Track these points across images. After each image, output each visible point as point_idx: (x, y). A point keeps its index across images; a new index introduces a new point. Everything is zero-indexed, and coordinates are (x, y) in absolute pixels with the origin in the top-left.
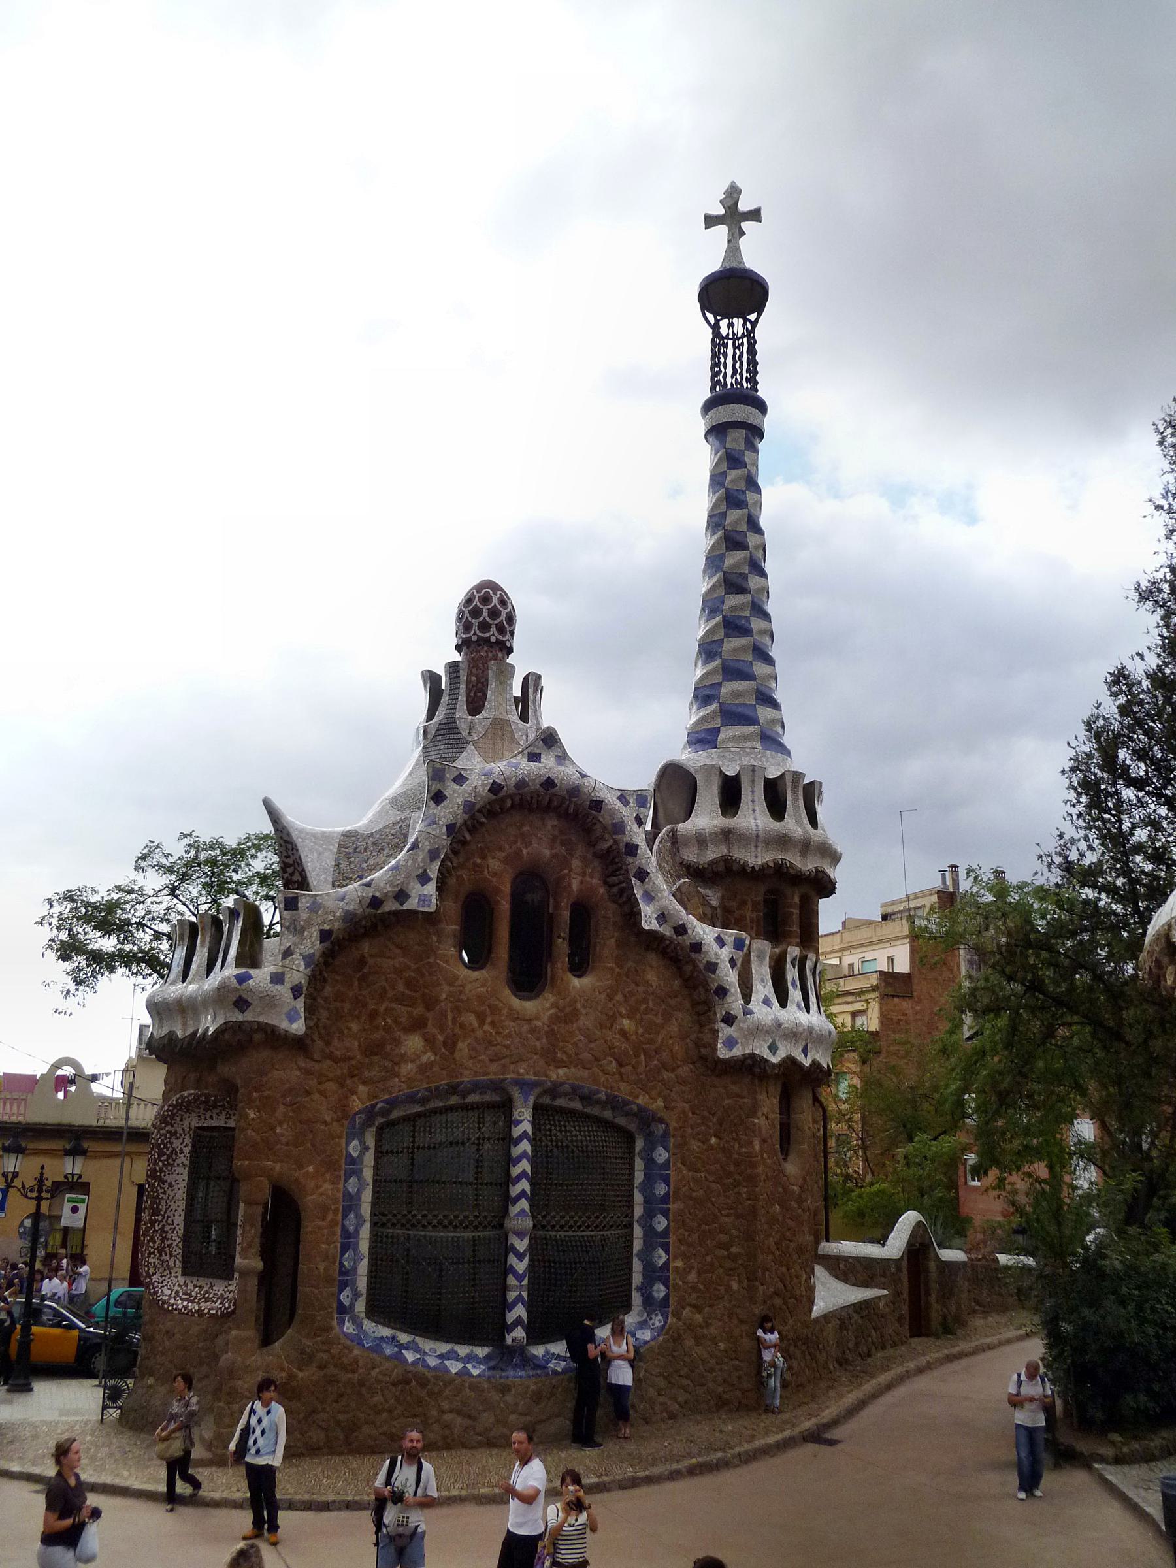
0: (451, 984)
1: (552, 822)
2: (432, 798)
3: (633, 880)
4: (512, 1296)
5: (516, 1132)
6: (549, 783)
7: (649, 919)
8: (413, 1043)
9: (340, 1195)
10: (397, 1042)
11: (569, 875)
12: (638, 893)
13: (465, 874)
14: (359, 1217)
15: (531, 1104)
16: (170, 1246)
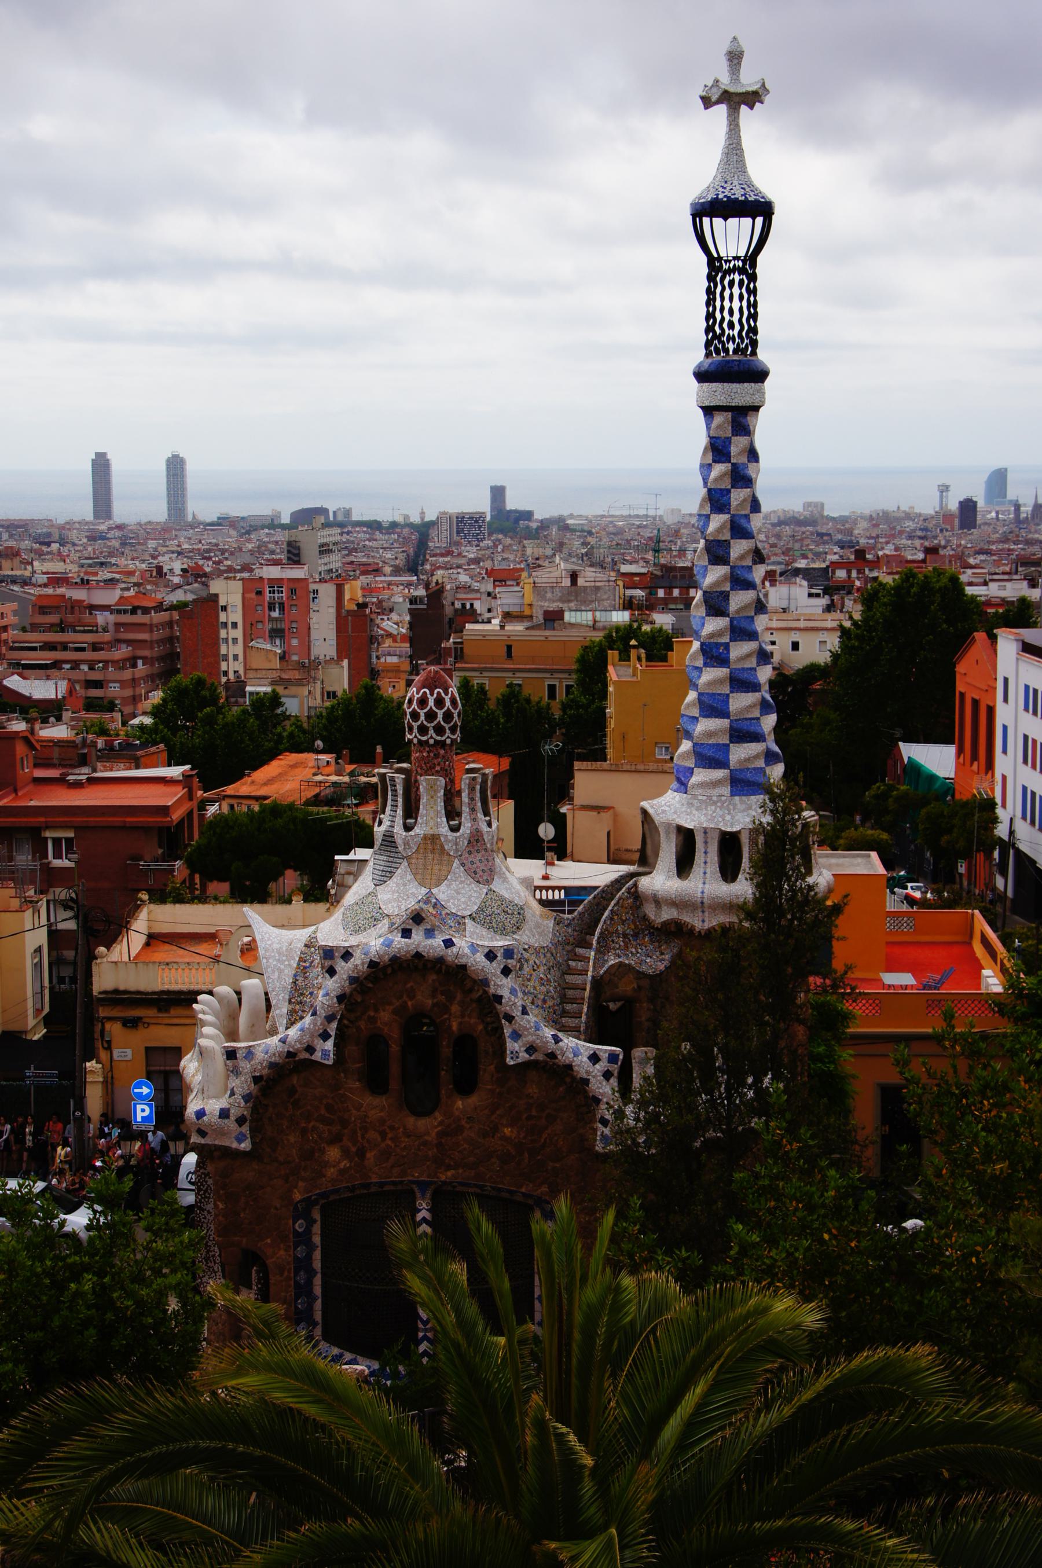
0: (358, 1110)
1: (432, 977)
2: (327, 972)
3: (503, 1021)
4: (421, 1334)
5: (419, 1216)
6: (418, 955)
7: (516, 1051)
8: (333, 1153)
9: (291, 1259)
10: (323, 1151)
11: (449, 1019)
12: (507, 1031)
13: (362, 1024)
14: (311, 1273)
15: (428, 1195)
16: (213, 1256)
